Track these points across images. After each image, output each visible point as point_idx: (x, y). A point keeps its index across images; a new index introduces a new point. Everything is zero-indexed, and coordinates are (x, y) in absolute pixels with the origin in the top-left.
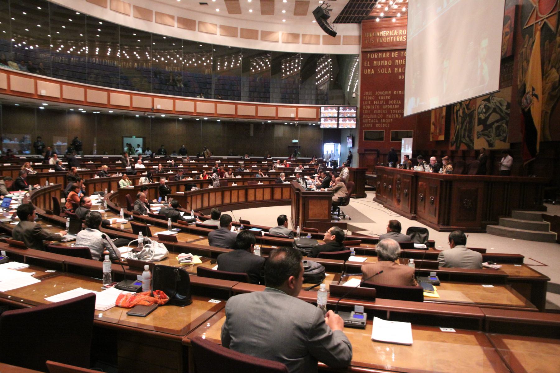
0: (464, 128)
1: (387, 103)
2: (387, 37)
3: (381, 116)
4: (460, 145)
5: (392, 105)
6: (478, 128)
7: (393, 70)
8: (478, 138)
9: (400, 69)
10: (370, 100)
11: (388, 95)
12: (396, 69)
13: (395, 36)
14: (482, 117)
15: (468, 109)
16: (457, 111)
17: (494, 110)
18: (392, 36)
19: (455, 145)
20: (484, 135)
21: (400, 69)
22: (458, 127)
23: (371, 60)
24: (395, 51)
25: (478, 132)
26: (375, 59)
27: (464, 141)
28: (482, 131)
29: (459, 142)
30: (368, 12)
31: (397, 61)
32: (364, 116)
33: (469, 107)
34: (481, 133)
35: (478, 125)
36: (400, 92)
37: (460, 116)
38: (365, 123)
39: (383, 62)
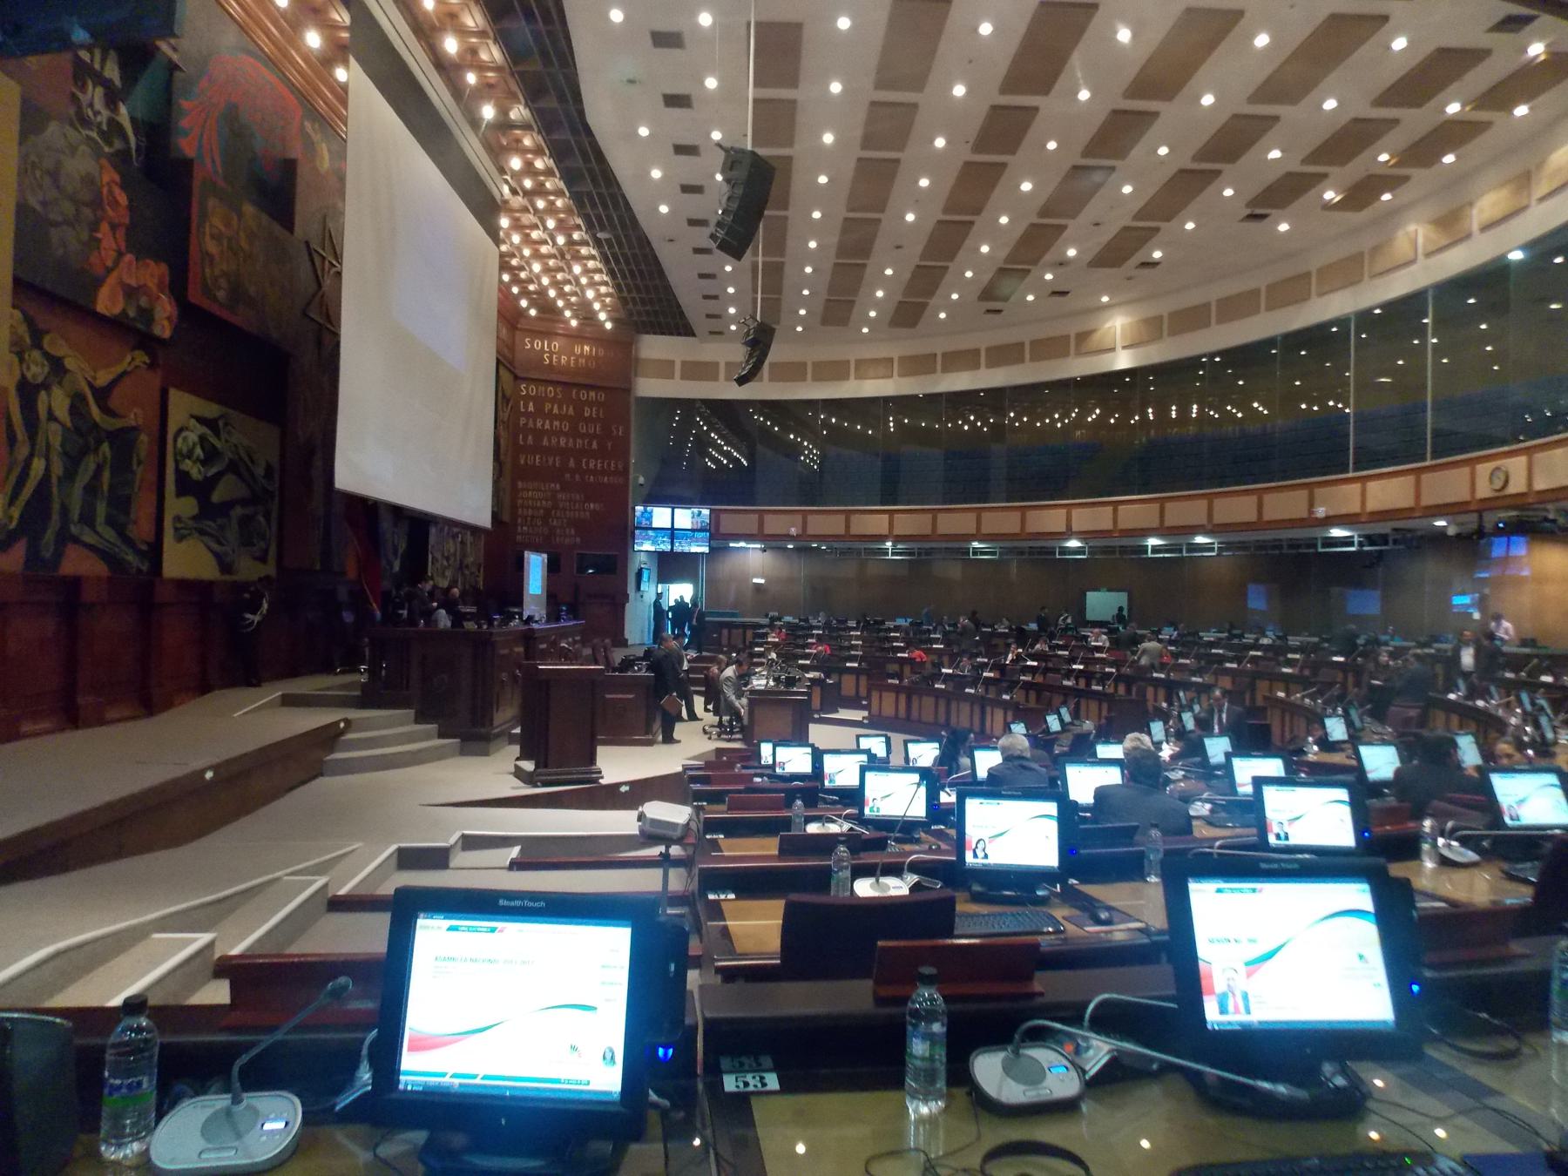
0: (83, 478)
4: (59, 555)
6: (180, 507)
8: (180, 538)
14: (195, 471)
15: (106, 410)
17: (233, 467)
19: (19, 551)
20: (202, 532)
22: (38, 466)
25: (178, 519)
27: (89, 538)
28: (194, 518)
29: (49, 535)
33: (115, 402)
34: (191, 523)
37: (52, 417)
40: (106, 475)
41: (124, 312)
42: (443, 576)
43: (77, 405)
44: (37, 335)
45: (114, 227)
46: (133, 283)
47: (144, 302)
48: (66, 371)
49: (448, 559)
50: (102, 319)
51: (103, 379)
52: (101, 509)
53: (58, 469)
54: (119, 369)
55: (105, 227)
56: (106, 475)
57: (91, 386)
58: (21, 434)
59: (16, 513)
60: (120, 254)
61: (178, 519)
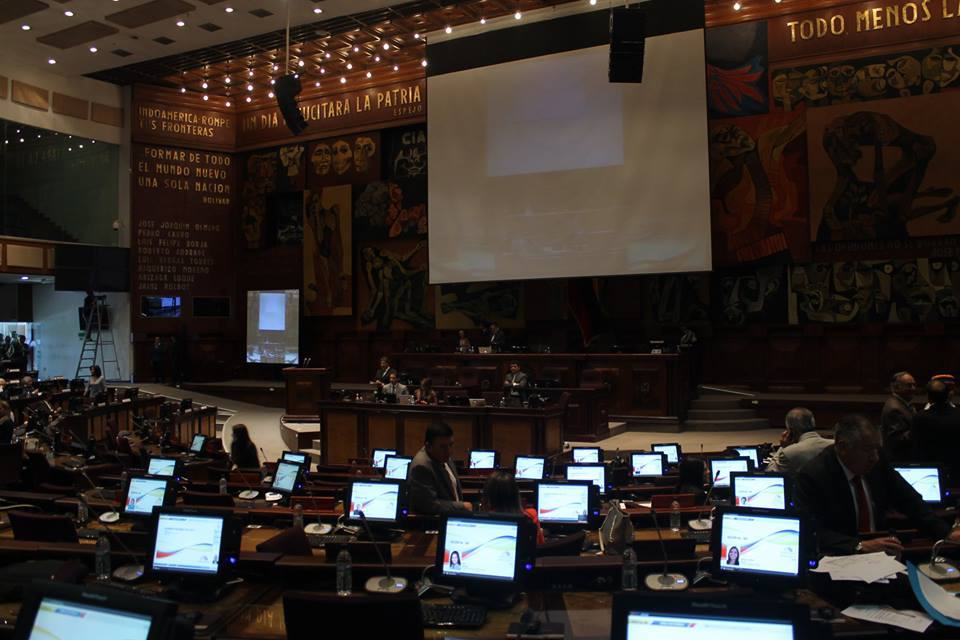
1: (184, 246)
2: (180, 123)
3: (174, 269)
5: (193, 249)
7: (192, 187)
9: (205, 185)
10: (150, 237)
11: (185, 230)
12: (198, 184)
13: (195, 124)
16: (375, 272)
18: (189, 123)
21: (205, 185)
22: (380, 294)
23: (152, 162)
24: (194, 150)
26: (159, 161)
30: (174, 73)
31: (198, 170)
32: (140, 268)
35: (443, 294)
36: (205, 226)
37: (384, 277)
38: (143, 282)
39: (173, 167)
40: (409, 293)
41: (402, 232)
42: (836, 308)
43: (395, 270)
44: (377, 253)
45: (395, 205)
46: (406, 219)
47: (412, 224)
48: (389, 260)
49: (850, 294)
50: (393, 238)
51: (405, 258)
52: (408, 306)
53: (388, 294)
54: (414, 251)
55: (392, 206)
56: (409, 293)
57: (400, 262)
58: (373, 286)
59: (373, 311)
60: (399, 212)
61: (444, 304)
